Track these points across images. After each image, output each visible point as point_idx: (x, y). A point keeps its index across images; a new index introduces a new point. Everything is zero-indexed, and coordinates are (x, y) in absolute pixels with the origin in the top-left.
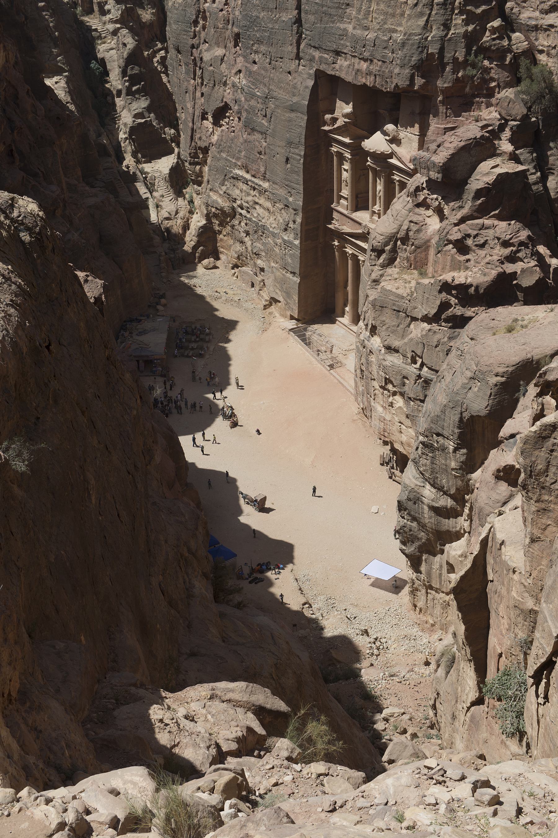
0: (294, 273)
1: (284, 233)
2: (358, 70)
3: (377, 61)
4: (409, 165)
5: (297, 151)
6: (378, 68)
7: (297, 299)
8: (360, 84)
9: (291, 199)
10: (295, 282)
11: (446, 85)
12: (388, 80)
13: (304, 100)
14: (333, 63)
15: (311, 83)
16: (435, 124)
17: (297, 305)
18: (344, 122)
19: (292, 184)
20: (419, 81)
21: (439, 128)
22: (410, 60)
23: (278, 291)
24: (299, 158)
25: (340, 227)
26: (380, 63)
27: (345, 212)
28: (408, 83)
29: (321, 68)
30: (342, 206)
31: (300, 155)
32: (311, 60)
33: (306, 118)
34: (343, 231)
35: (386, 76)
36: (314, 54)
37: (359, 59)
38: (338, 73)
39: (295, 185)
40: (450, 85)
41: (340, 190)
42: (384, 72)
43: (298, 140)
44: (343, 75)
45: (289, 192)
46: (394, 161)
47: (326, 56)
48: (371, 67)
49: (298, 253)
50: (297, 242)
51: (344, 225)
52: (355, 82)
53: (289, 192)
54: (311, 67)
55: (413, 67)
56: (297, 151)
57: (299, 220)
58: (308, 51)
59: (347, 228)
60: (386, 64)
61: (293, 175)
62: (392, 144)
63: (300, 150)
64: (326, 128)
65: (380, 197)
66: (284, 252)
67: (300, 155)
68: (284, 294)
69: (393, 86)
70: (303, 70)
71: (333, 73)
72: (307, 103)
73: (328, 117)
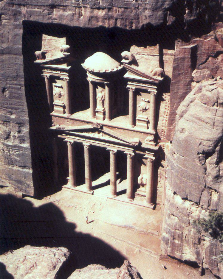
0: (24, 167)
1: (6, 141)
2: (92, 17)
3: (117, 9)
4: (155, 77)
5: (15, 82)
6: (120, 14)
7: (32, 184)
8: (95, 27)
9: (13, 117)
10: (28, 173)
11: (192, 18)
12: (133, 21)
13: (17, 45)
14: (49, 14)
15: (21, 31)
16: (180, 46)
17: (33, 187)
18: (64, 55)
19: (13, 106)
20: (171, 20)
21: (186, 48)
22: (162, 5)
23: (4, 180)
24: (19, 87)
25: (62, 126)
26: (123, 9)
27: (65, 115)
28: (161, 21)
29: (32, 19)
30: (57, 111)
31: (20, 85)
32: (15, 15)
33: (22, 57)
34: (65, 129)
35: (133, 18)
36: (18, 9)
37: (91, 8)
38: (56, 22)
39: (17, 106)
40: (195, 17)
41: (52, 100)
42: (127, 16)
43: (15, 74)
44: (65, 22)
45: (10, 112)
46: (127, 75)
47: (37, 9)
48: (110, 13)
49: (29, 153)
50: (26, 145)
51: (62, 124)
52: (87, 26)
53: (10, 112)
54: (16, 20)
55: (166, 10)
56: (15, 82)
57: (26, 130)
58: (11, 8)
59: (68, 126)
60: (129, 10)
61: (13, 99)
62: (131, 65)
63: (20, 81)
64: (38, 61)
65: (103, 102)
66: (8, 153)
67: (20, 85)
68: (14, 182)
69: (140, 25)
70: (7, 22)
71: (50, 22)
72: (21, 46)
73: (37, 53)
